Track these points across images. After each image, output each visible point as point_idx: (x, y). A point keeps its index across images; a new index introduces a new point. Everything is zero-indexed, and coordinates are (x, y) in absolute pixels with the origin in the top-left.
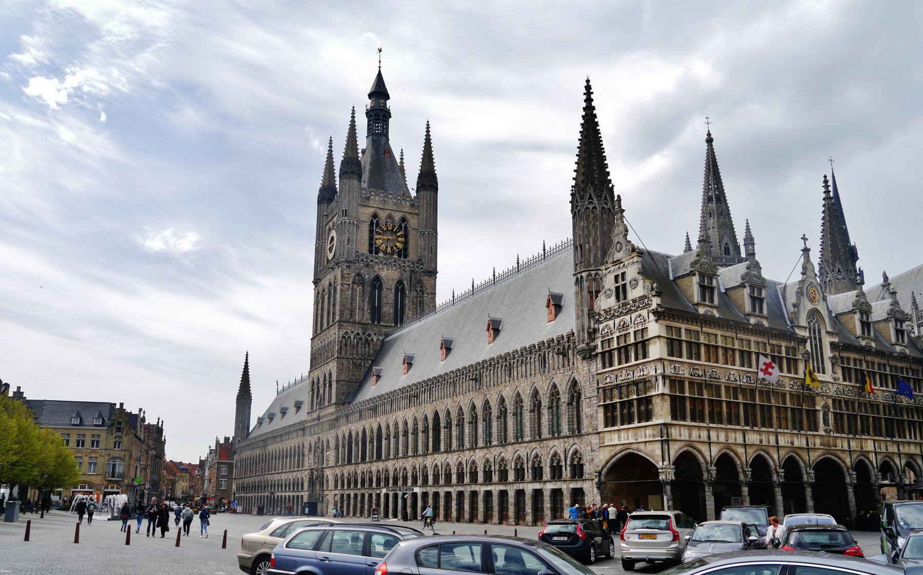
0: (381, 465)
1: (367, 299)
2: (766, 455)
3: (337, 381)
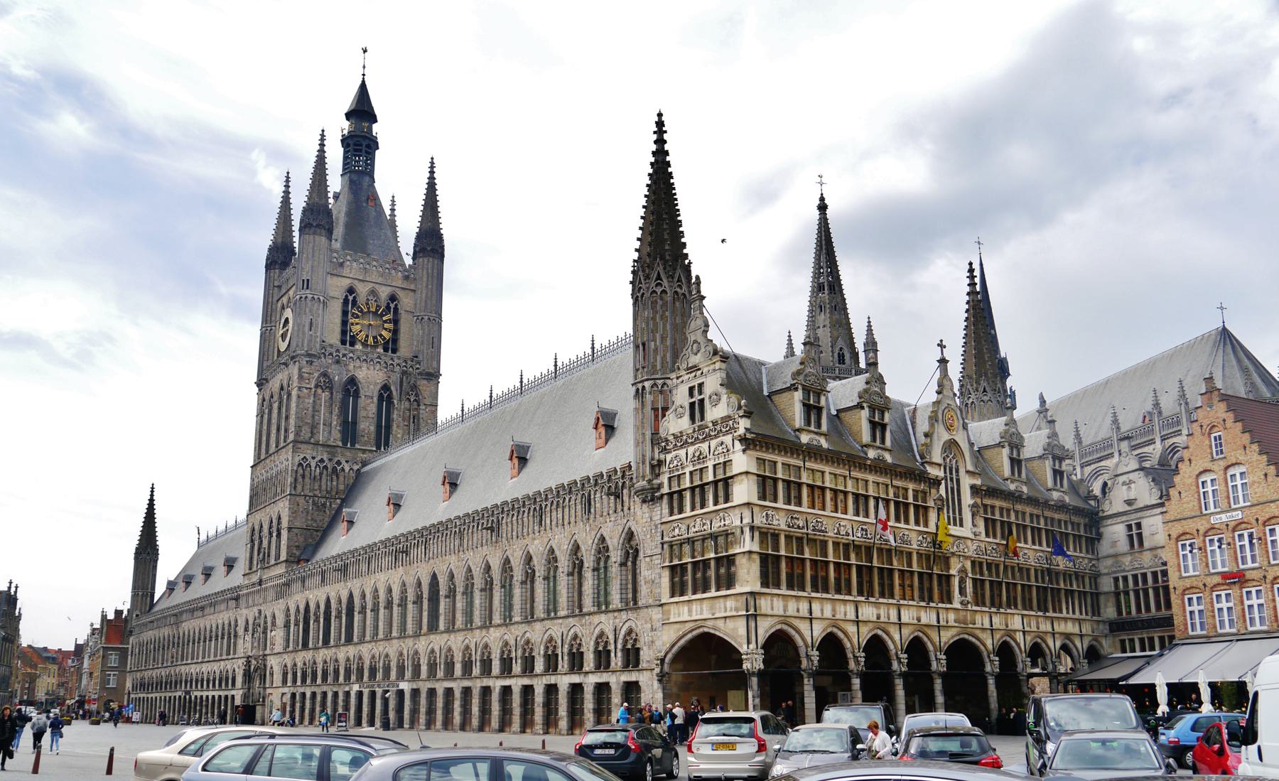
0: (351, 651)
1: (336, 411)
2: (884, 636)
3: (290, 529)
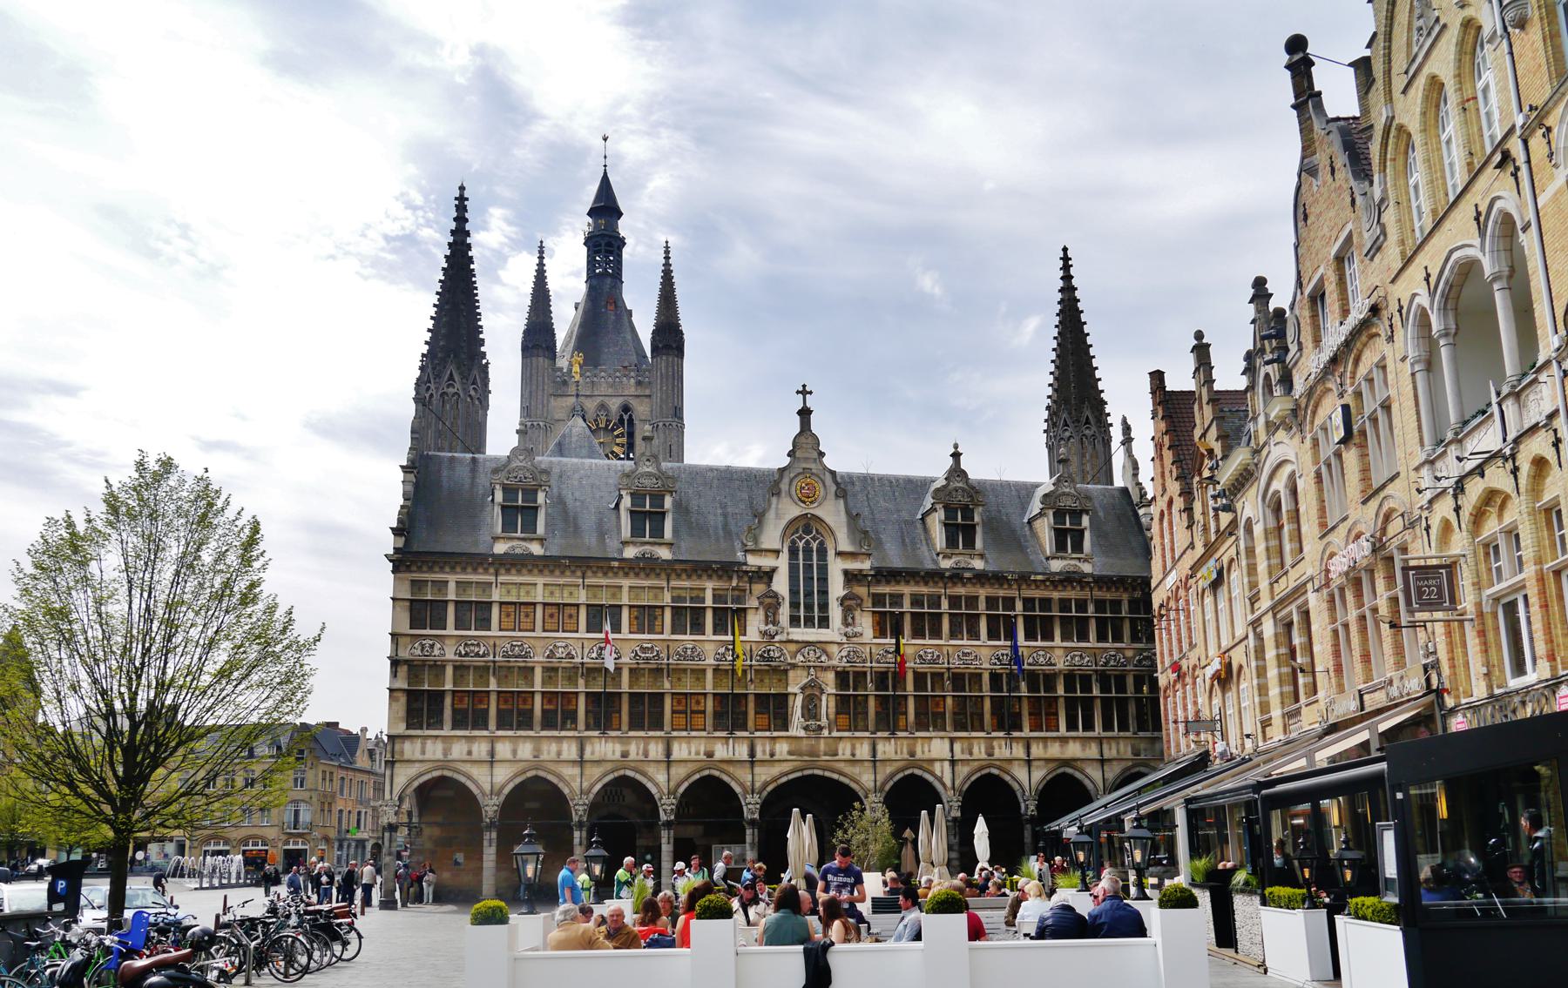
2: (639, 777)
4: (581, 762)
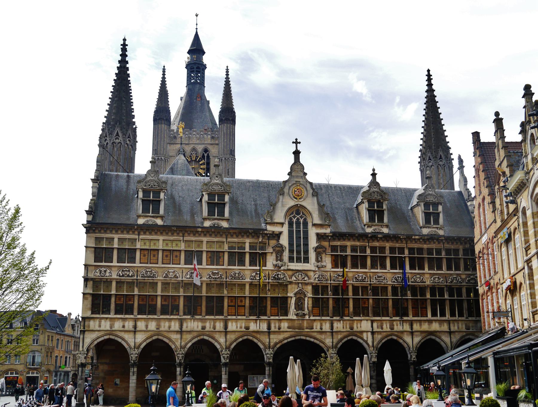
2: (210, 340)
4: (181, 332)
